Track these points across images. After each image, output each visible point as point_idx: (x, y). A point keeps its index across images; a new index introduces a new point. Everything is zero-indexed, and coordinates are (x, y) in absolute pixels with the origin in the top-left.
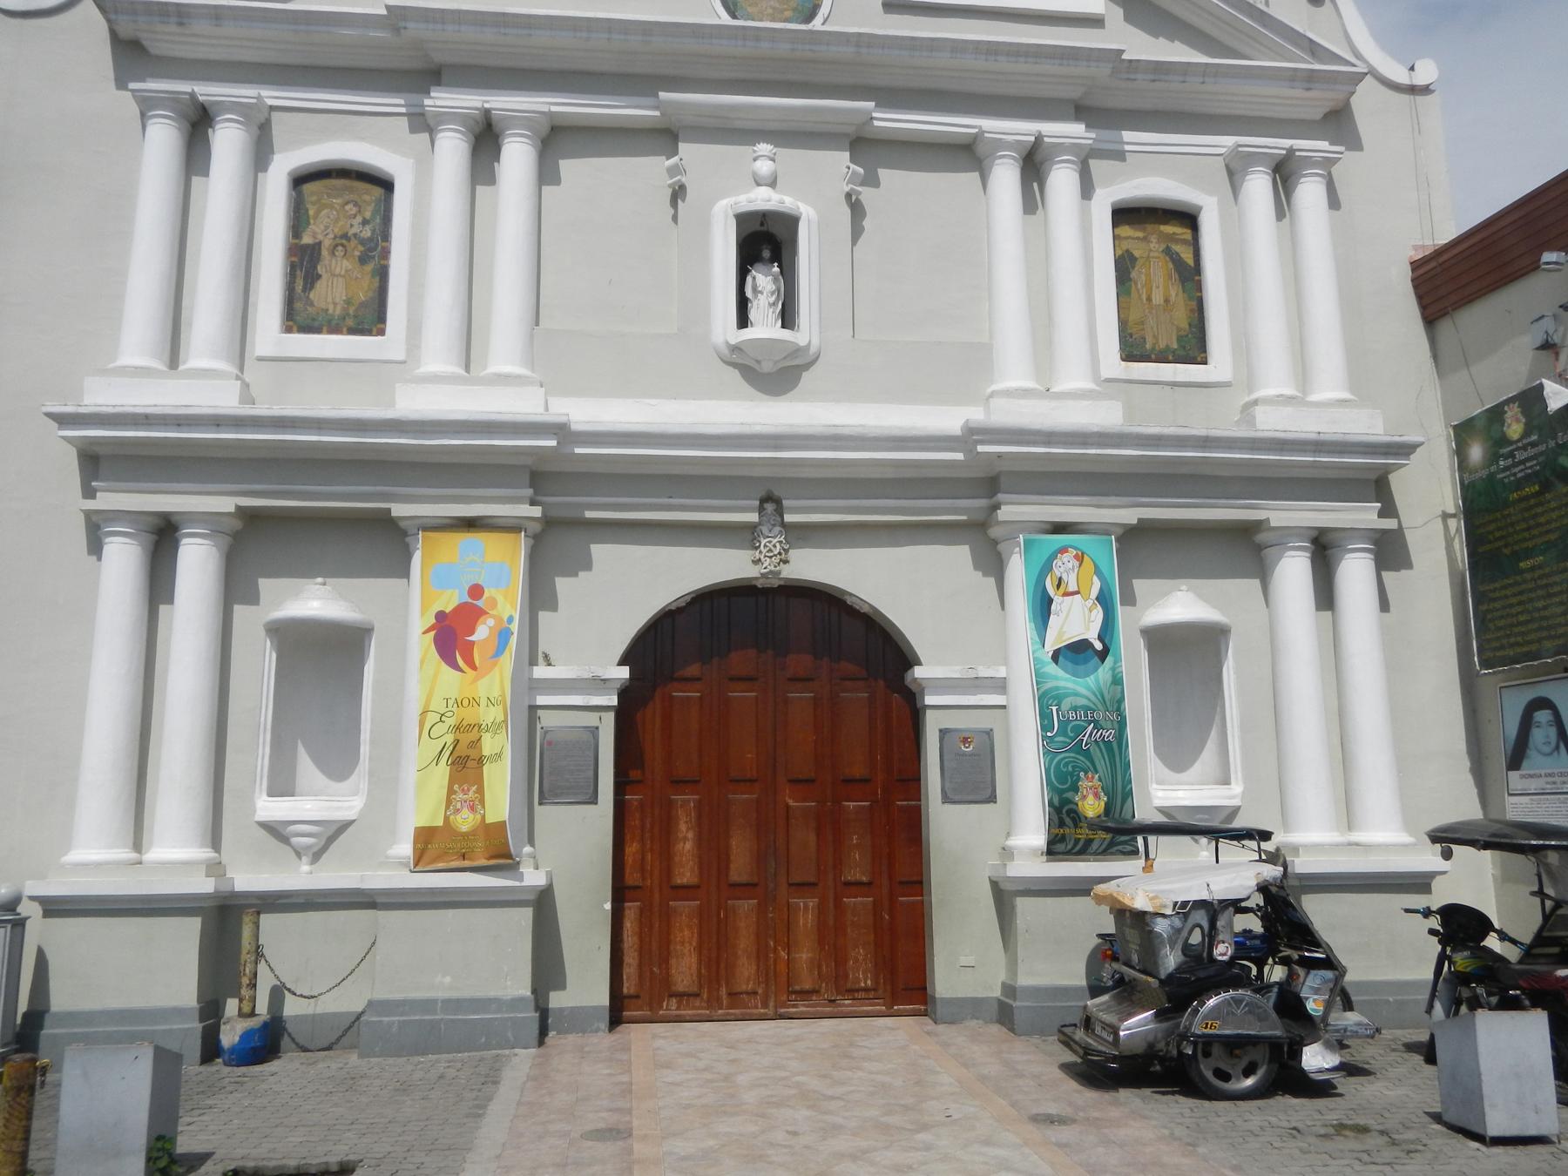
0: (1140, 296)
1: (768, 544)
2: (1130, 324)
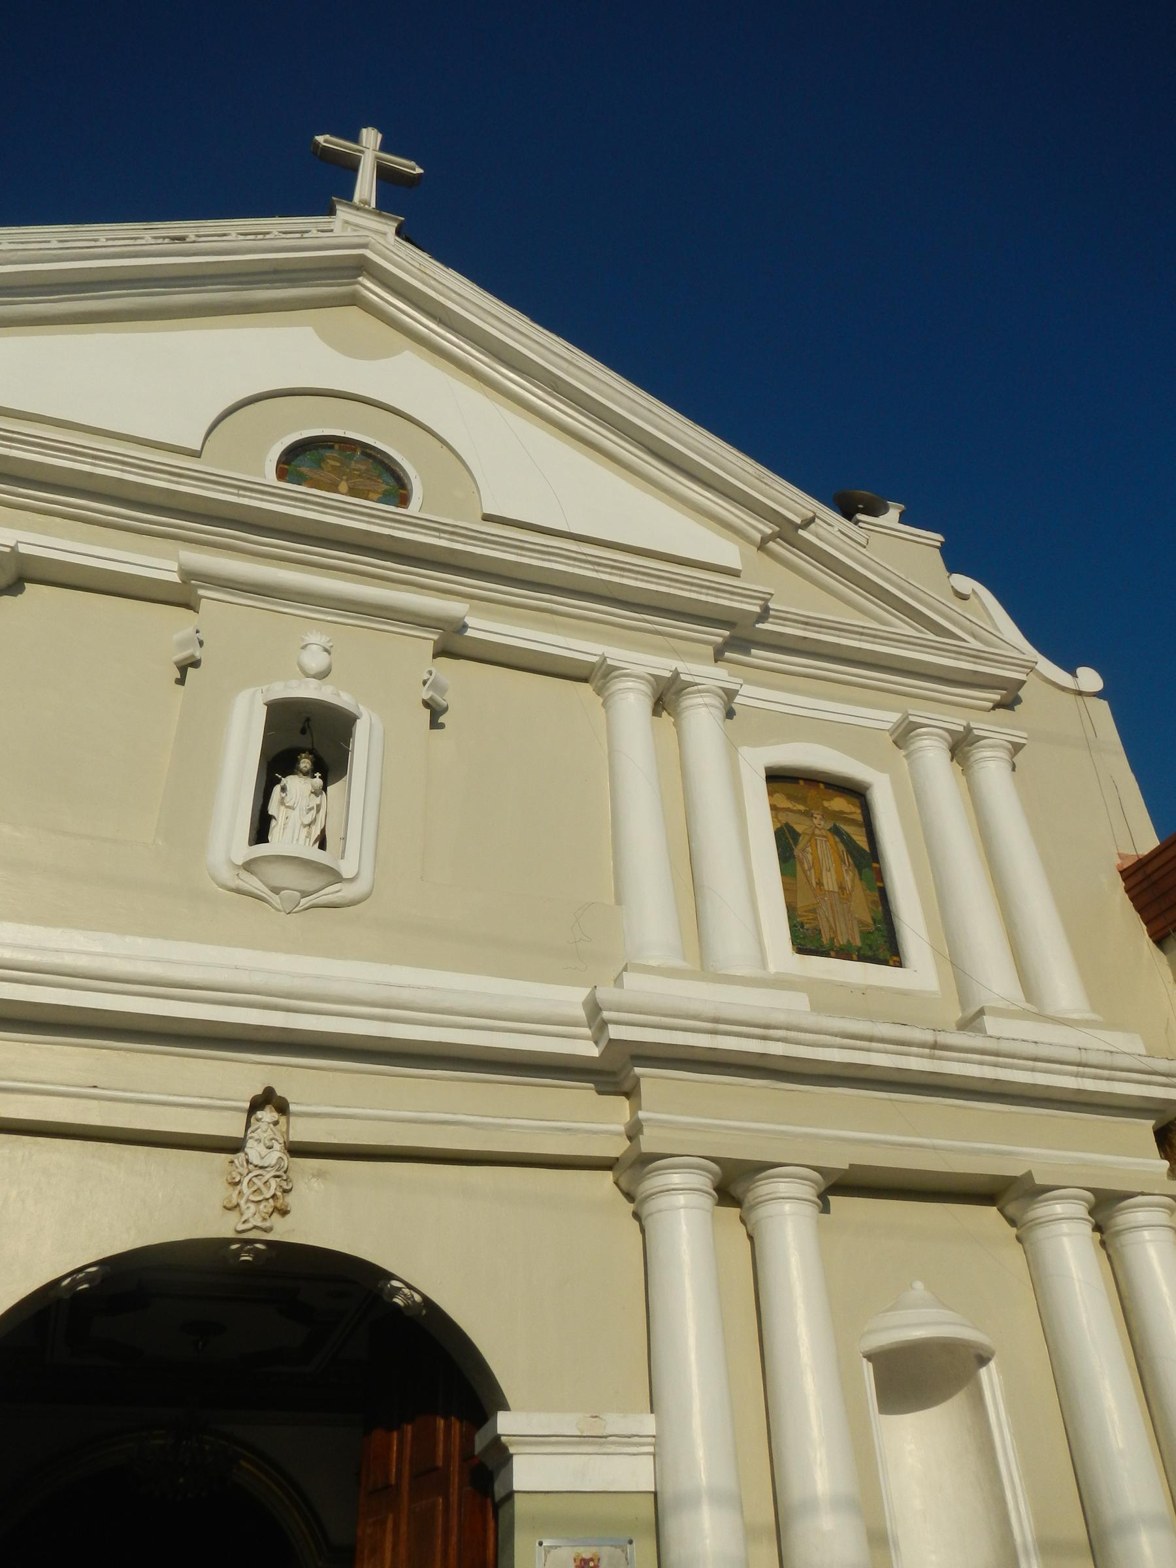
1: (254, 1179)
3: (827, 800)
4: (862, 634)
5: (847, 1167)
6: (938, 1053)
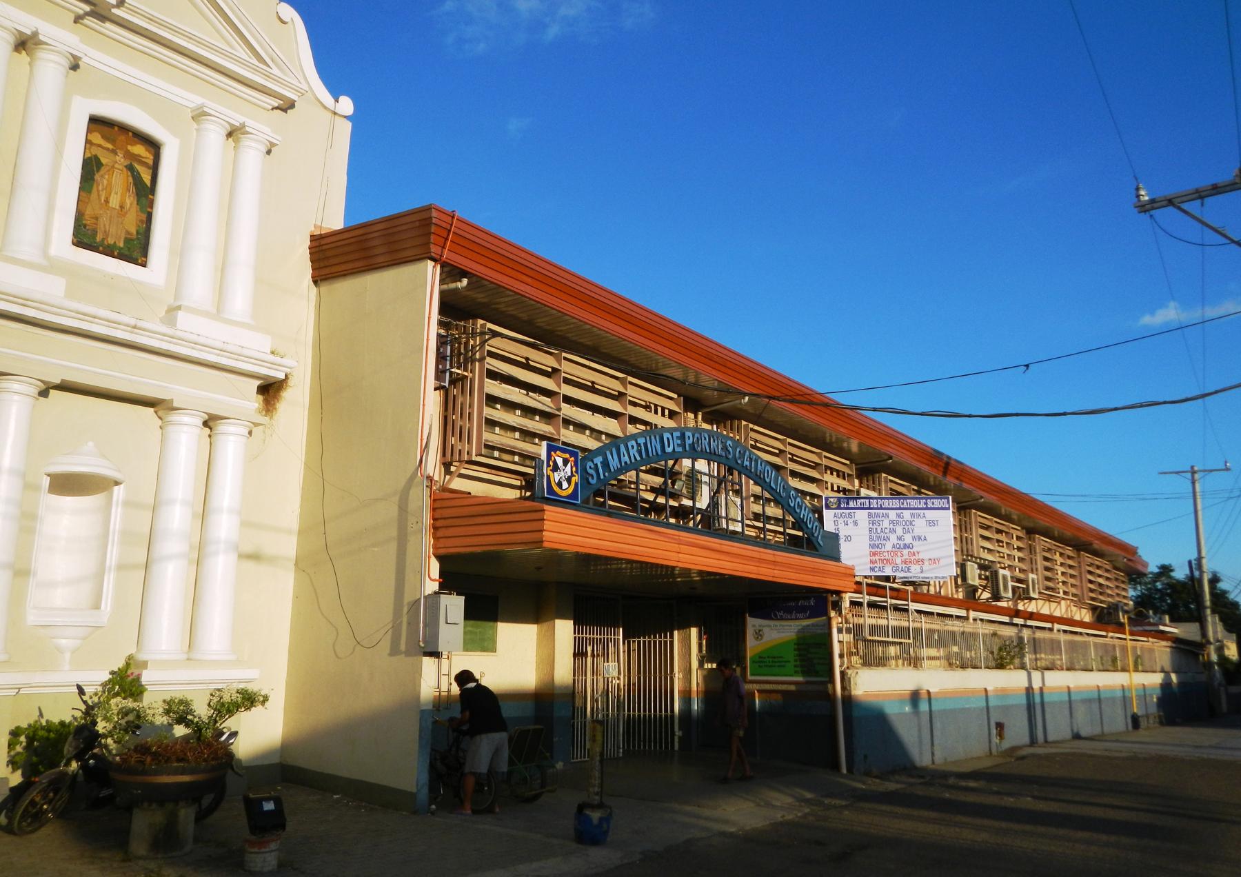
0: (99, 196)
2: (87, 217)
3: (131, 145)
4: (191, 38)
5: (59, 382)
6: (136, 330)
